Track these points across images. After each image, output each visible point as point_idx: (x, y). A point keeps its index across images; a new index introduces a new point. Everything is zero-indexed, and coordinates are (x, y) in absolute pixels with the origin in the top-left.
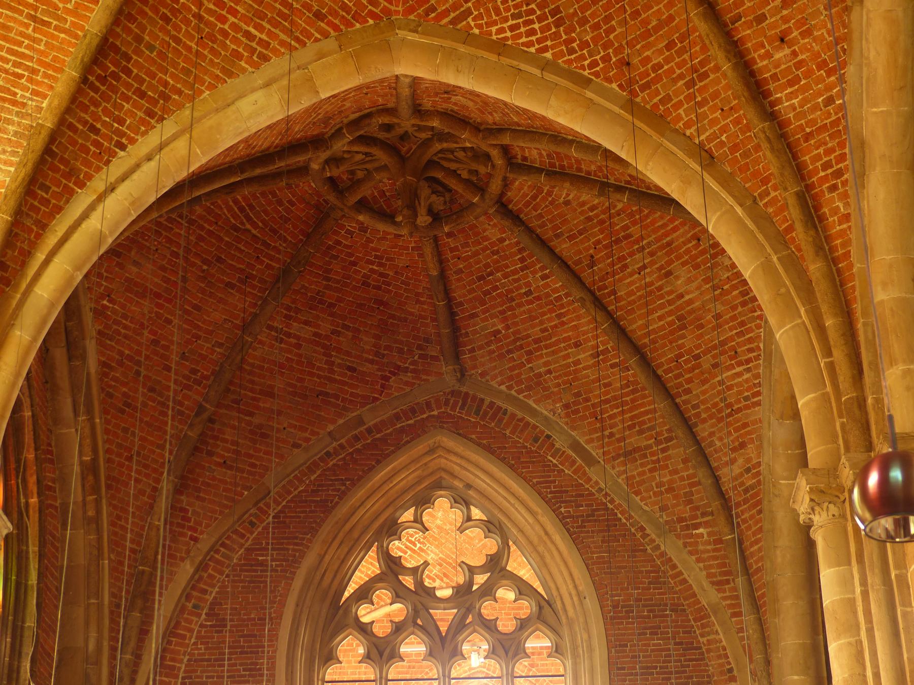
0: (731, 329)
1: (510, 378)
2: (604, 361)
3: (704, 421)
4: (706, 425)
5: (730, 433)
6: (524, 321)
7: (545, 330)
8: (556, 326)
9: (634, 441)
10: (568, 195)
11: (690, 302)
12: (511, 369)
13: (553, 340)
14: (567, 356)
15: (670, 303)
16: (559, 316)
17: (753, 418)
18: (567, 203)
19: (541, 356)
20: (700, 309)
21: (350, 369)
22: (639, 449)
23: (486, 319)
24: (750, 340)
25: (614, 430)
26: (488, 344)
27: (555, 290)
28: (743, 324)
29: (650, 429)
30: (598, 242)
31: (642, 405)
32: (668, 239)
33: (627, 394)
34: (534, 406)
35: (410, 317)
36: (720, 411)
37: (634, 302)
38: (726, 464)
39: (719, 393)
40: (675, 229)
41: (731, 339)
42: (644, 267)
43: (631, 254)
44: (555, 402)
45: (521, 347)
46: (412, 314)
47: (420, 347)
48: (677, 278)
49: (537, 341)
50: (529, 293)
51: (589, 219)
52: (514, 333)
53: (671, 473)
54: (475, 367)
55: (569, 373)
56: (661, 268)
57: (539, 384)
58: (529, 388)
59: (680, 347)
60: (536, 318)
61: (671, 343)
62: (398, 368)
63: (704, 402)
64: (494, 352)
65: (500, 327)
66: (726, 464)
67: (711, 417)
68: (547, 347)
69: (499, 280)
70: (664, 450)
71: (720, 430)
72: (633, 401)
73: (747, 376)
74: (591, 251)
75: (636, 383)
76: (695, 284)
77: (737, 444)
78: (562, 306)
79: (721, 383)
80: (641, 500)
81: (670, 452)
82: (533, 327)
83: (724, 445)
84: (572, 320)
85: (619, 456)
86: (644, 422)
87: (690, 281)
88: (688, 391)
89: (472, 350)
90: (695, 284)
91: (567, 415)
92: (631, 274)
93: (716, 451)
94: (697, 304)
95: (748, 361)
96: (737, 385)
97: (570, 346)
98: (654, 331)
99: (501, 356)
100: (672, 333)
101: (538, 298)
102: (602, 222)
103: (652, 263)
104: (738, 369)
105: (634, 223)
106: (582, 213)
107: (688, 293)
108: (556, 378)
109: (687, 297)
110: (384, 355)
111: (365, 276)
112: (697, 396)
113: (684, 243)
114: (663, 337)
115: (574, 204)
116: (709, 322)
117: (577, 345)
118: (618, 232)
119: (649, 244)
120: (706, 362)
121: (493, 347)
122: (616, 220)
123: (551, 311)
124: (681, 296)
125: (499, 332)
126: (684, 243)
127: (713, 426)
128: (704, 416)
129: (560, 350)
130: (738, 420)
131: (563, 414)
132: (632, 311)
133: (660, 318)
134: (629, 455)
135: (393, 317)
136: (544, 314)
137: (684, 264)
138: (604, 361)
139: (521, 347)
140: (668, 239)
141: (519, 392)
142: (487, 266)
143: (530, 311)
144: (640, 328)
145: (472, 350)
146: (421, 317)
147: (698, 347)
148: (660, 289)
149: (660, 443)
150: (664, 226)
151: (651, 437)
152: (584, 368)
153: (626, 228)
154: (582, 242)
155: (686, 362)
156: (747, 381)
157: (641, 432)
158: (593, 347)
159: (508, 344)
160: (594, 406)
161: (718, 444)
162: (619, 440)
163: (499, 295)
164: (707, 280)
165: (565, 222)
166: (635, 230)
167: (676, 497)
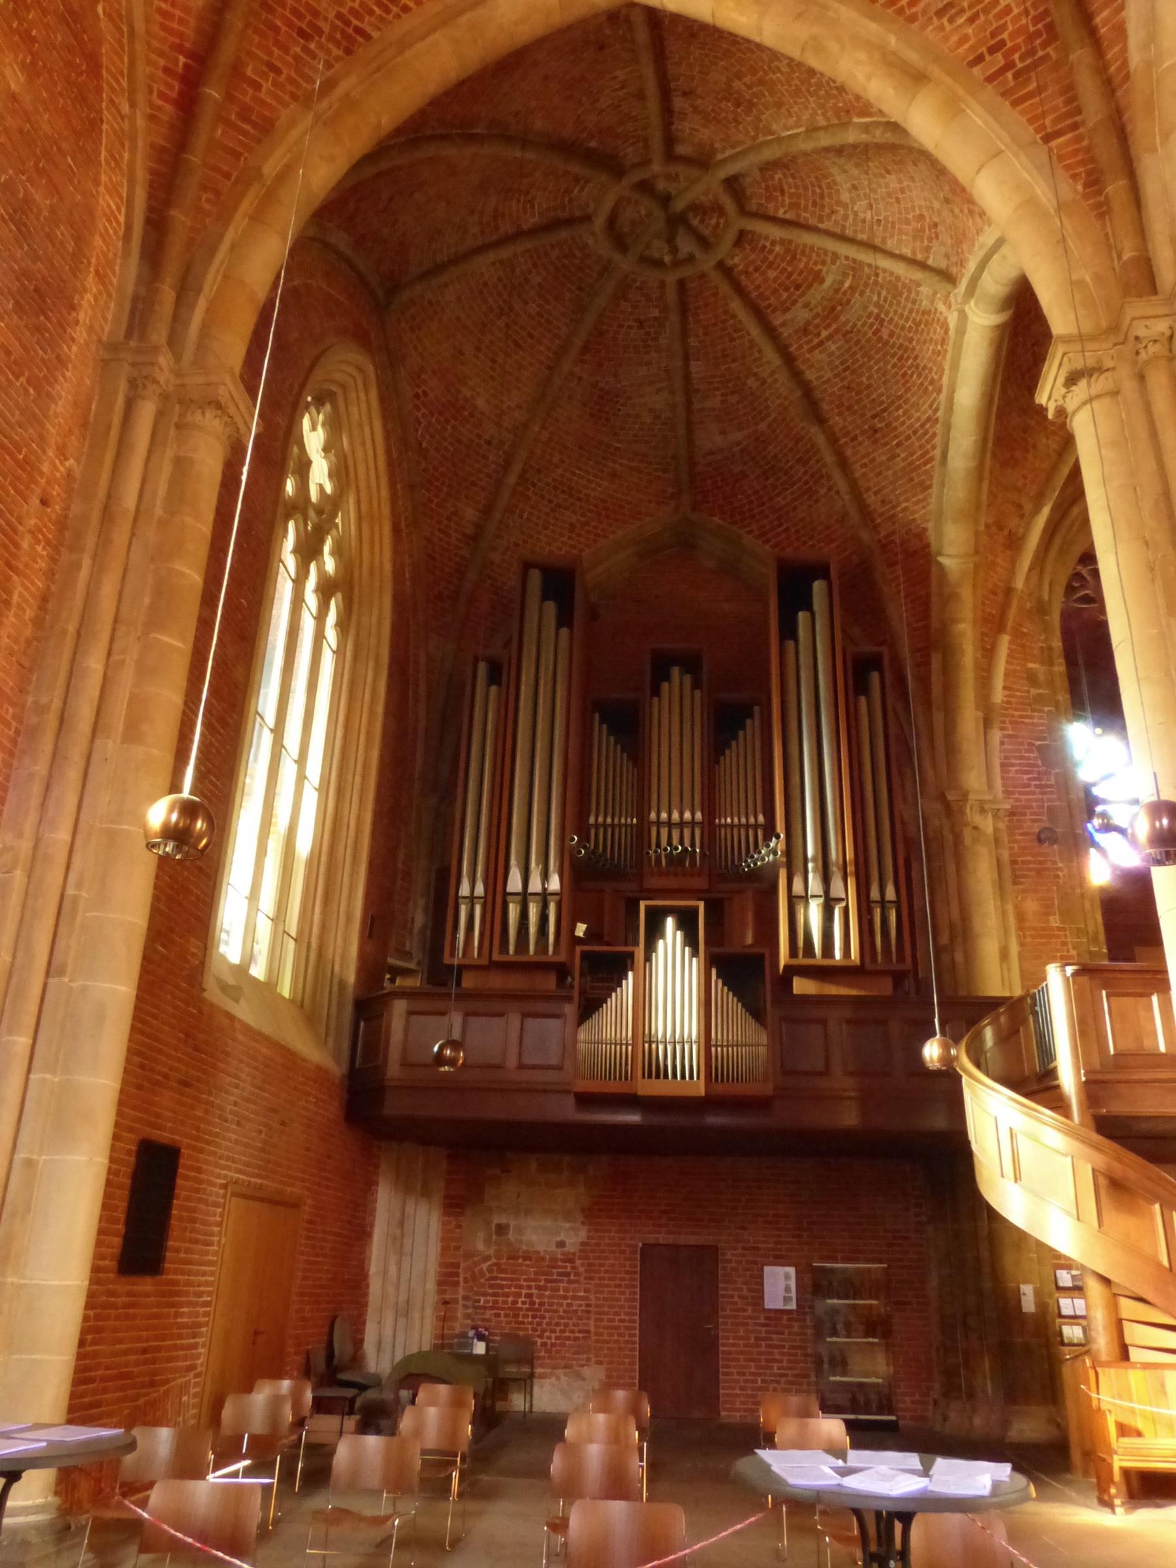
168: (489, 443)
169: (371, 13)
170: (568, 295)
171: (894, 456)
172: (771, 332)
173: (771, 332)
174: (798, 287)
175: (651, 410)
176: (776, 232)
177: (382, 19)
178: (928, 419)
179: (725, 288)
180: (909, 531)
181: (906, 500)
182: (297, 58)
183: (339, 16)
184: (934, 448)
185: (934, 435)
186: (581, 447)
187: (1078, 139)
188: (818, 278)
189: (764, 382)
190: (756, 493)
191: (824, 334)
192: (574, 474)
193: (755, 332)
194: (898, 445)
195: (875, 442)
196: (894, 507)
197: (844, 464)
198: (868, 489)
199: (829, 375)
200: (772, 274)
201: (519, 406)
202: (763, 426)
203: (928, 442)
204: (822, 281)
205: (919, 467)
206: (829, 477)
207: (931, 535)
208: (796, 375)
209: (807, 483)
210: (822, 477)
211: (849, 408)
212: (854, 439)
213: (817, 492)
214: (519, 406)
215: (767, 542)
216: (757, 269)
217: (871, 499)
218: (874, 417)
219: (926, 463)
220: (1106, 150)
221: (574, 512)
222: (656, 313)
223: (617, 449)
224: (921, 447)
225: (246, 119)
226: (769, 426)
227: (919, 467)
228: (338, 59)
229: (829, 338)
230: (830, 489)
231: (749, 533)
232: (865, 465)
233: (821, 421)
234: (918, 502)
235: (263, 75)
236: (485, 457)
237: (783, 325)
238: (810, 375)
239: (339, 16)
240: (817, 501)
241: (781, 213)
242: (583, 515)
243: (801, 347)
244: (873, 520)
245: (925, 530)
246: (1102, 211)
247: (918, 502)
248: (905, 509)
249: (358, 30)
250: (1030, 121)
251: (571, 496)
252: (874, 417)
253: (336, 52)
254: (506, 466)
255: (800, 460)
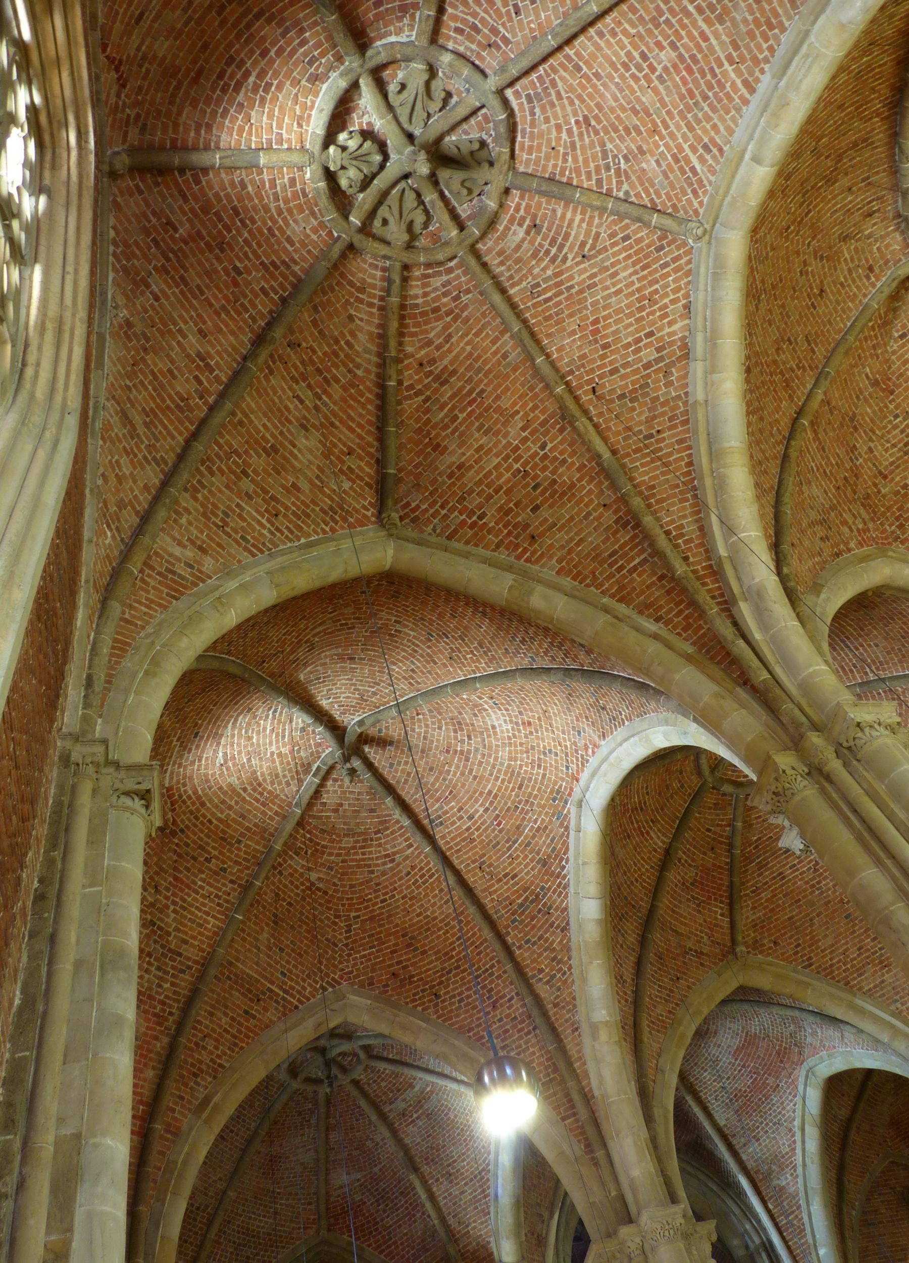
0: (293, 504)
1: (127, 245)
2: (198, 367)
3: (196, 499)
4: (192, 502)
5: (202, 532)
6: (199, 262)
7: (202, 293)
8: (211, 305)
9: (138, 419)
10: (361, 320)
11: (296, 457)
12: (136, 244)
13: (194, 302)
14: (186, 323)
15: (281, 433)
16: (224, 308)
17: (233, 551)
18: (351, 318)
19: (170, 287)
20: (294, 468)
21: (141, 15)
22: (135, 429)
23: (184, 213)
24: (300, 529)
25: (134, 390)
26: (154, 213)
27: (254, 307)
28: (308, 516)
29: (153, 434)
30: (314, 352)
31: (170, 420)
32: (337, 423)
33: (173, 401)
34: (110, 279)
35: (175, 110)
36: (216, 516)
37: (268, 395)
38: (174, 539)
39: (229, 507)
40: (350, 429)
41: (287, 508)
42: (302, 402)
43: (309, 386)
44: (126, 307)
45: (168, 259)
46: (179, 113)
47: (138, 116)
48: (307, 438)
49: (182, 278)
50: (236, 268)
51: (337, 342)
52: (180, 249)
53: (131, 473)
54: (122, 193)
55: (165, 325)
56: (305, 418)
57: (135, 283)
58: (125, 270)
59: (246, 452)
60: (209, 277)
61: (247, 442)
62: (124, 86)
63: (210, 491)
64: (149, 221)
65: (181, 231)
66: (174, 539)
67: (202, 505)
68: (182, 292)
69: (240, 234)
70: (145, 458)
71: (196, 519)
72: (168, 407)
73: (265, 532)
74: (304, 345)
75: (191, 410)
76: (312, 458)
77: (199, 543)
78: (239, 314)
79: (238, 505)
80: (101, 447)
81: (148, 468)
82: (199, 275)
83: (187, 530)
84: (223, 322)
85: (118, 403)
86: (156, 427)
87: (311, 452)
88: (212, 473)
89: (140, 192)
90: (312, 458)
91: (121, 327)
92: (290, 388)
93: (175, 521)
94: (296, 463)
95: (278, 529)
96: (249, 524)
97: (196, 324)
98: (251, 422)
99: (146, 232)
100: (257, 442)
101: (236, 284)
102: (336, 355)
103: (307, 409)
104: (264, 521)
105: (344, 388)
106: (342, 333)
107: (300, 451)
108: (152, 306)
109: (296, 451)
110: (141, 66)
111: (242, 62)
112: (213, 484)
113: (340, 440)
114: (248, 432)
115: (352, 326)
116: (287, 481)
117: (200, 331)
118: (329, 371)
119: (326, 405)
120: (246, 485)
121: (154, 220)
122: (342, 369)
123: (226, 297)
124: (294, 446)
125: (176, 230)
126: (340, 440)
127: (196, 510)
128: (199, 496)
129: (187, 312)
130: (219, 537)
131: (120, 320)
132: (260, 395)
133: (264, 426)
134: (125, 418)
135: (178, 88)
136: (220, 291)
137: (320, 441)
138: (198, 367)
139: (168, 259)
140: (337, 423)
141: (115, 254)
142: (253, 221)
143: (216, 271)
144: (248, 405)
145: (140, 192)
146: (176, 125)
147: (255, 472)
148: (289, 422)
149: (150, 453)
150: (353, 420)
151: (149, 440)
152: (179, 343)
153: (337, 381)
154: (312, 334)
155: (235, 462)
156: (261, 535)
157: (146, 425)
158: (208, 353)
159: (163, 240)
160: (143, 359)
161: (183, 521)
162: (129, 399)
163: (220, 232)
164: (319, 468)
165: (330, 316)
166: (336, 391)
167: (118, 490)
168: (198, 1208)
169: (225, 1054)
170: (257, 1104)
171: (463, 1193)
172: (383, 1116)
173: (383, 1116)
174: (399, 1091)
175: (302, 1164)
176: (389, 1068)
177: (230, 1056)
178: (483, 1170)
179: (355, 1093)
180: (478, 1244)
181: (475, 1222)
182: (192, 1088)
183: (212, 1060)
184: (489, 1188)
185: (488, 1180)
186: (256, 1198)
187: (577, 1121)
188: (412, 1086)
189: (377, 1144)
190: (372, 1215)
191: (415, 1116)
192: (250, 1218)
193: (374, 1118)
194: (466, 1184)
195: (451, 1182)
196: (467, 1226)
197: (432, 1197)
198: (449, 1214)
199: (419, 1140)
200: (383, 1084)
201: (220, 1179)
202: (376, 1170)
203: (485, 1183)
204: (413, 1087)
205: (480, 1200)
206: (423, 1206)
207: (493, 1245)
208: (399, 1141)
209: (407, 1208)
210: (417, 1205)
211: (433, 1160)
212: (437, 1180)
213: (414, 1215)
214: (220, 1179)
215: (381, 1253)
216: (375, 1082)
217: (451, 1221)
218: (449, 1165)
219: (485, 1197)
220: (591, 1132)
221: (250, 1247)
222: (310, 1106)
223: (279, 1193)
224: (481, 1186)
225: (167, 1131)
226: (380, 1170)
227: (480, 1200)
228: (210, 1083)
229: (418, 1118)
230: (424, 1213)
231: (369, 1246)
232: (445, 1198)
233: (416, 1170)
234: (482, 1223)
235: (176, 1103)
236: (195, 1220)
237: (390, 1111)
238: (407, 1141)
239: (212, 1060)
240: (415, 1221)
241: (391, 1056)
242: (255, 1248)
243: (401, 1124)
244: (454, 1236)
245: (489, 1243)
246: (596, 1164)
247: (482, 1223)
248: (475, 1228)
249: (220, 1065)
250: (554, 1109)
251: (248, 1235)
252: (449, 1165)
253: (210, 1079)
254: (209, 1224)
255: (402, 1193)
